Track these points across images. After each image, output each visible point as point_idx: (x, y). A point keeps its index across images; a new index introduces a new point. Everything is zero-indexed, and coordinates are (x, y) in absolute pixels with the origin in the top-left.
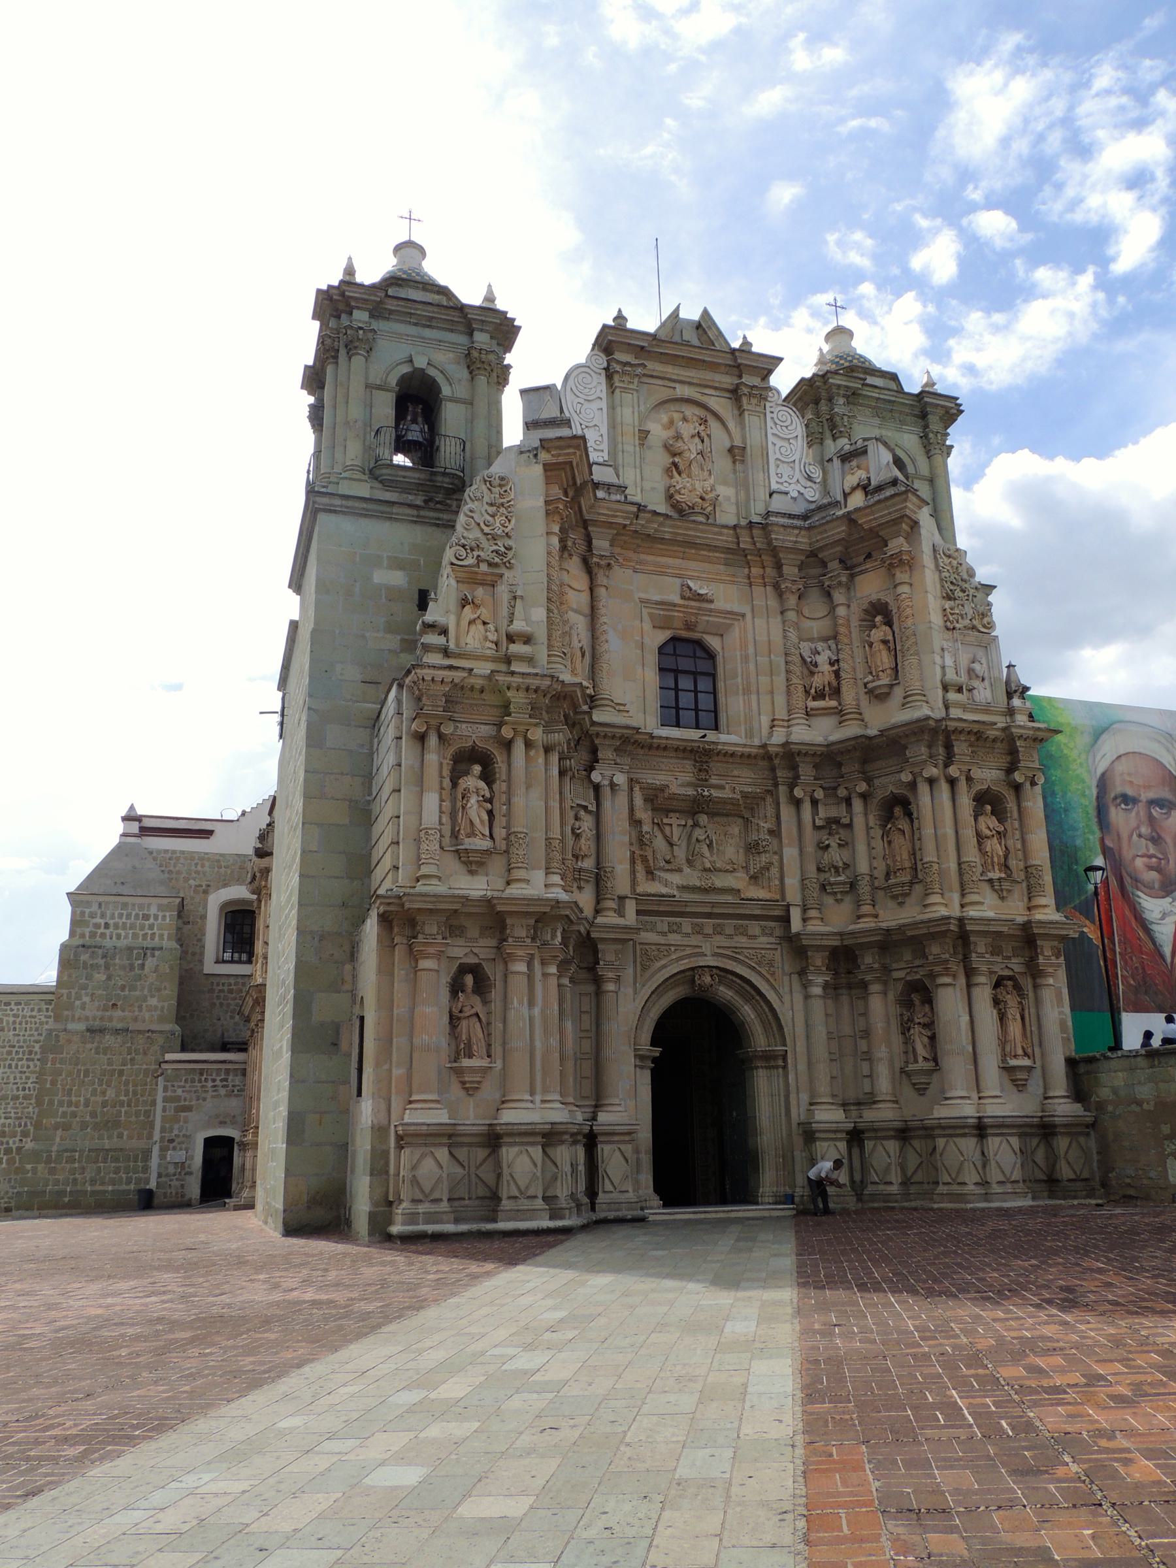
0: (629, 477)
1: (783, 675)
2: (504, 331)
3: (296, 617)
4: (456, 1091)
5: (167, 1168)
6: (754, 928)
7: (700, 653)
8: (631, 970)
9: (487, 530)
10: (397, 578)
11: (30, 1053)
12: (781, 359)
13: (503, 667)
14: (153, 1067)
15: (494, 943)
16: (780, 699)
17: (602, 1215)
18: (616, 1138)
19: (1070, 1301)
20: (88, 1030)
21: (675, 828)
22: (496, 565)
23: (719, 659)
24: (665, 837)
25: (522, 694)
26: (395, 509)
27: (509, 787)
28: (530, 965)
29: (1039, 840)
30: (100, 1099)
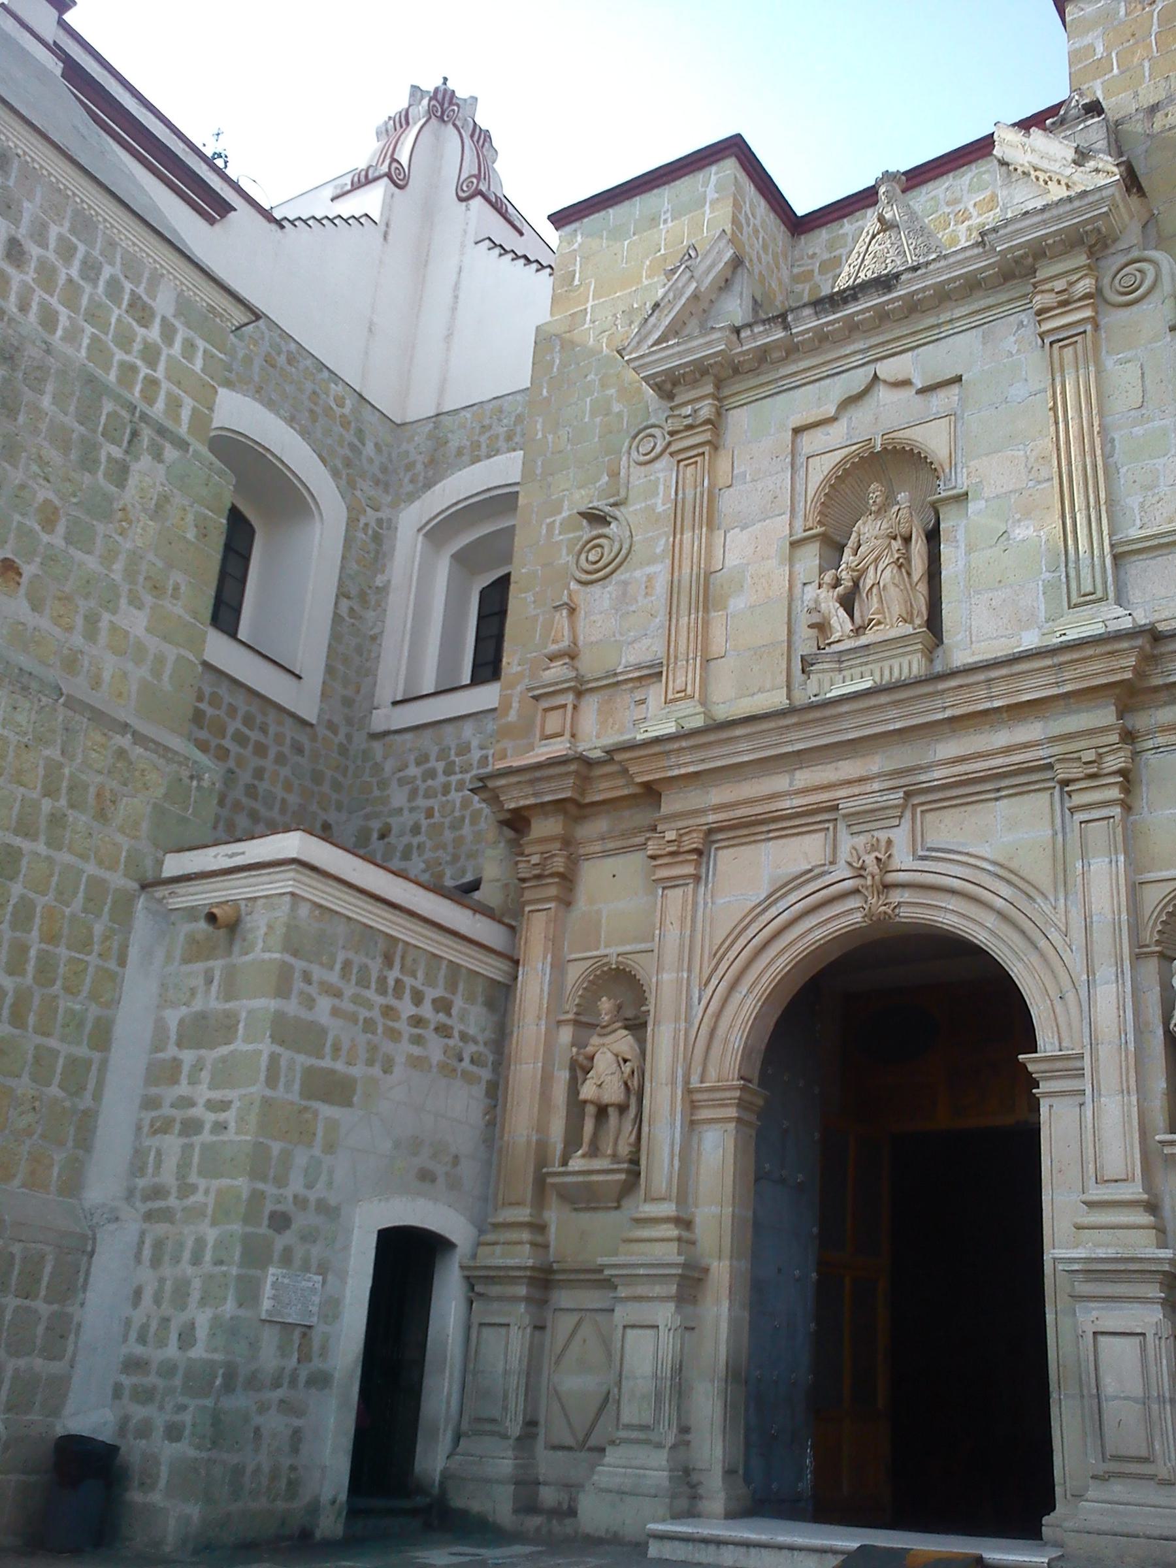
14: (119, 880)
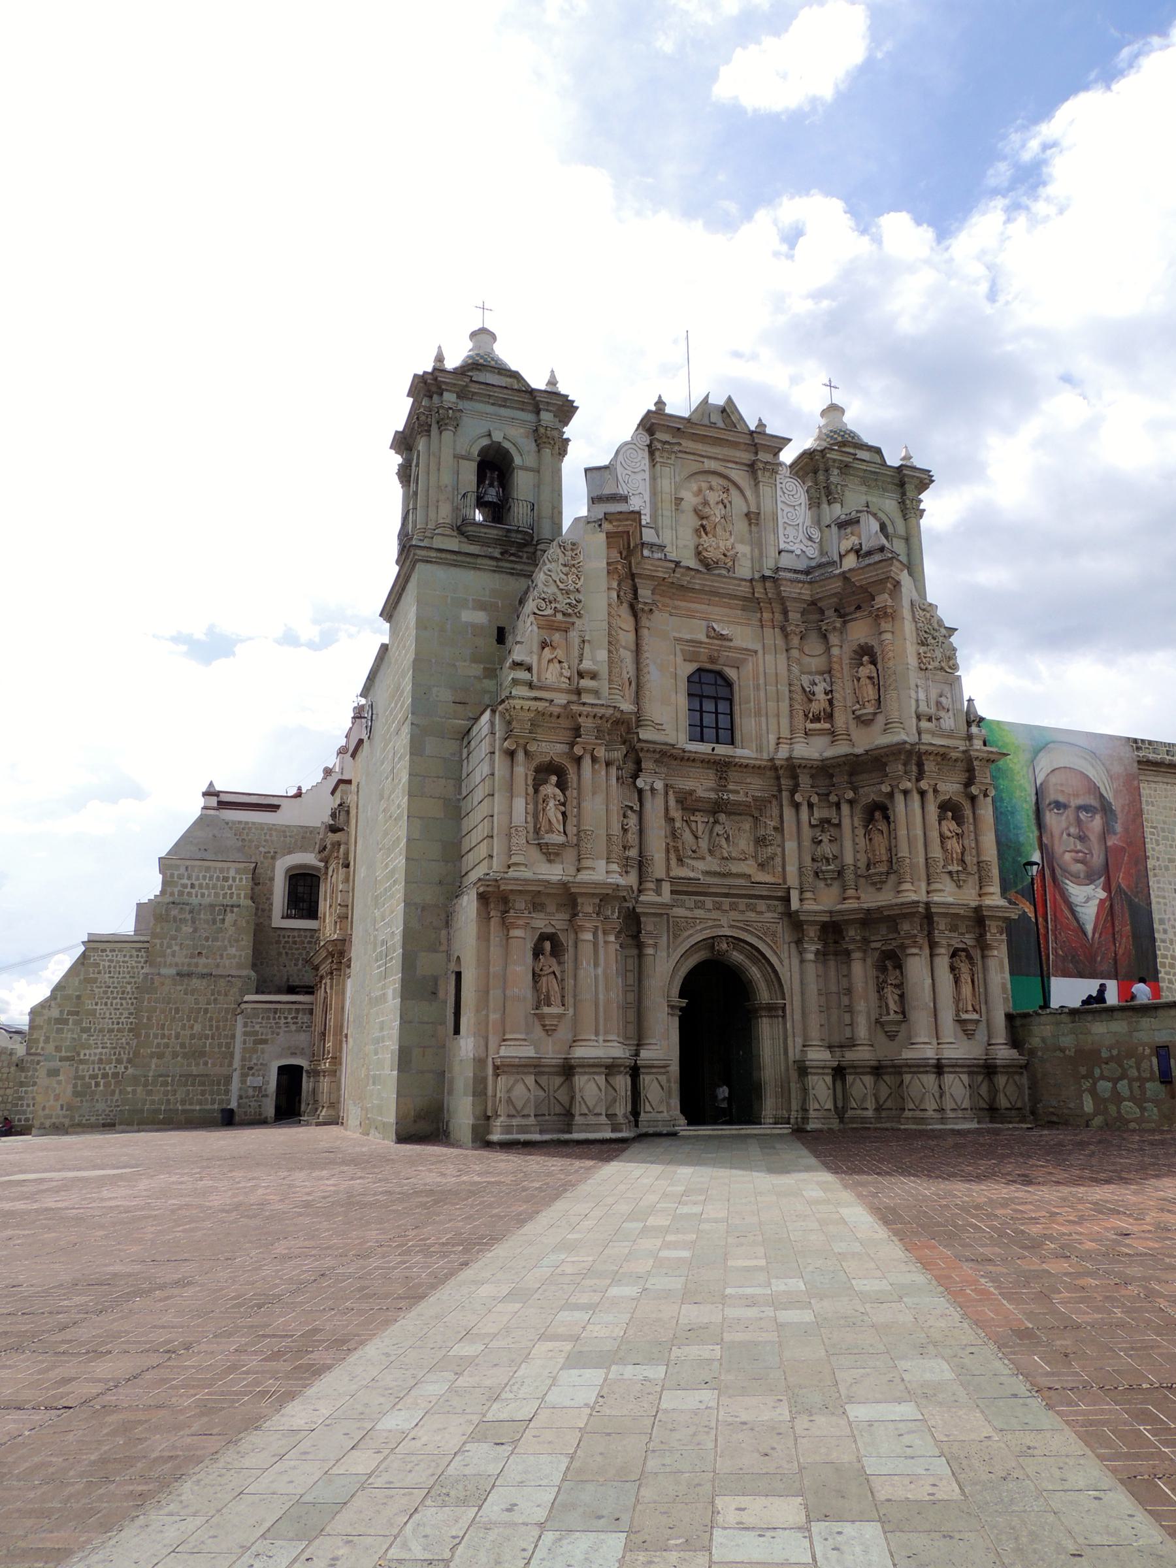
0: (667, 537)
1: (787, 701)
2: (565, 409)
3: (387, 642)
4: (538, 1032)
5: (247, 1091)
6: (762, 905)
7: (720, 681)
8: (665, 938)
9: (562, 586)
10: (480, 617)
11: (123, 993)
12: (790, 440)
13: (574, 698)
15: (567, 917)
16: (785, 722)
17: (644, 1130)
18: (654, 1070)
19: (1027, 1181)
20: (178, 974)
21: (699, 824)
22: (569, 615)
23: (736, 688)
24: (692, 831)
25: (590, 720)
26: (479, 561)
27: (579, 794)
28: (595, 934)
29: (989, 841)
30: (188, 1032)
